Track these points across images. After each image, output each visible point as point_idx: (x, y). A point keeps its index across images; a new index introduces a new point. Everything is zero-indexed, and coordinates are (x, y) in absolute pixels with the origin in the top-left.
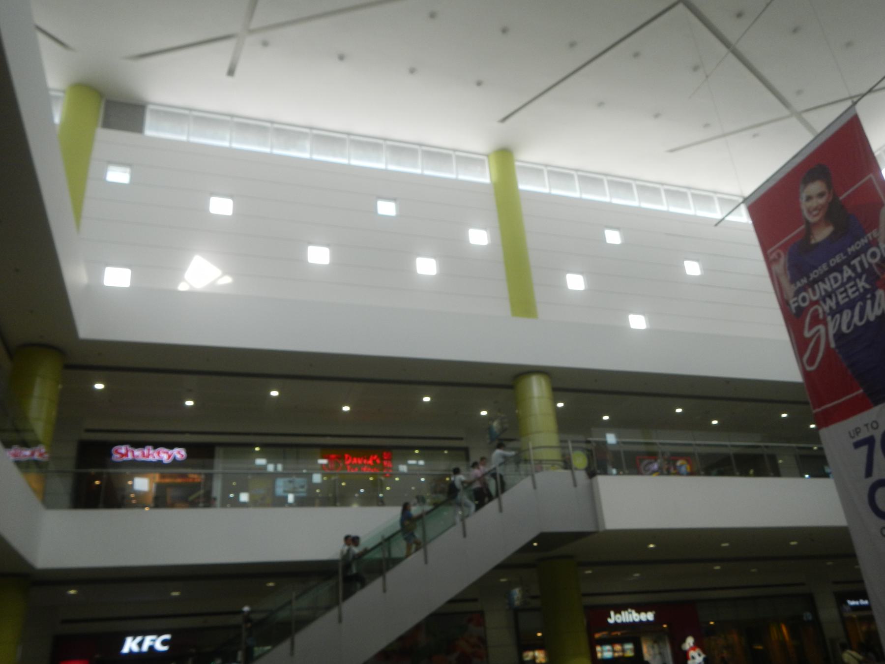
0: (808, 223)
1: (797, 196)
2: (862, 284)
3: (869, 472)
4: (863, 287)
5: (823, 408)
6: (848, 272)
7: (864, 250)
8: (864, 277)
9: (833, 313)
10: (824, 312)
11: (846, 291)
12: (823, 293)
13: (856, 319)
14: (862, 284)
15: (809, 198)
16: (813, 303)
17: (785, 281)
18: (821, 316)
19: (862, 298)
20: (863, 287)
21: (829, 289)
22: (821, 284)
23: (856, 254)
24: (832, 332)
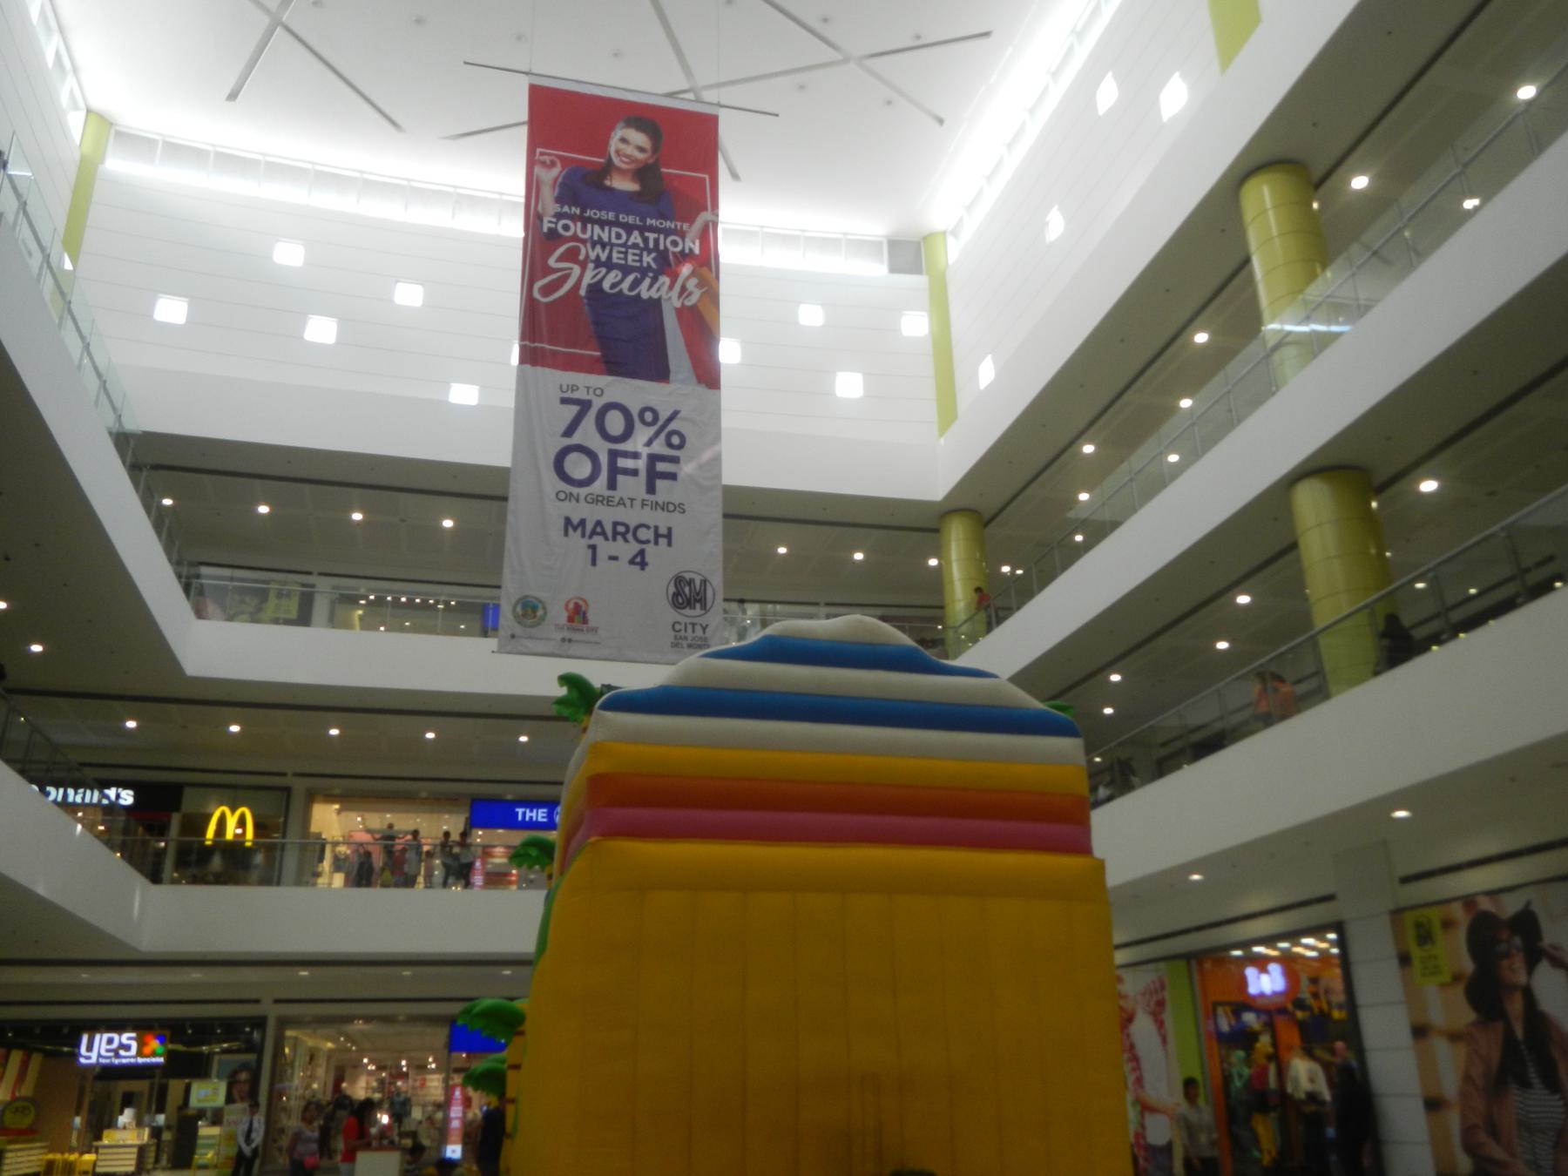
0: (610, 160)
1: (612, 128)
2: (648, 259)
3: (569, 432)
4: (648, 263)
5: (536, 344)
6: (636, 238)
7: (667, 232)
8: (653, 255)
10: (587, 256)
11: (626, 253)
12: (596, 238)
13: (625, 286)
14: (648, 259)
15: (624, 140)
16: (575, 238)
17: (548, 195)
18: (582, 257)
19: (644, 271)
20: (648, 263)
21: (606, 239)
22: (597, 229)
23: (652, 229)
24: (587, 280)
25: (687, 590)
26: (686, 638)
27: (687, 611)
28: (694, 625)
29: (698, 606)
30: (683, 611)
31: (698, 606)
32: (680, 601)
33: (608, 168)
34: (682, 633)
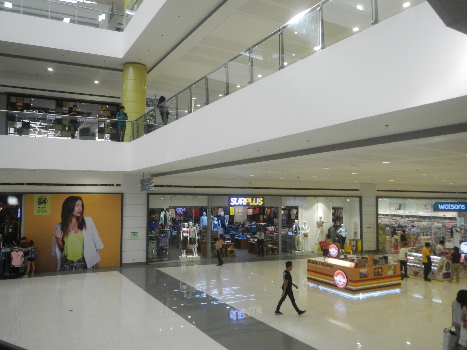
25: (41, 200)
26: (41, 210)
27: (41, 205)
28: (43, 207)
29: (44, 203)
30: (41, 205)
31: (44, 203)
32: (40, 203)
34: (40, 210)
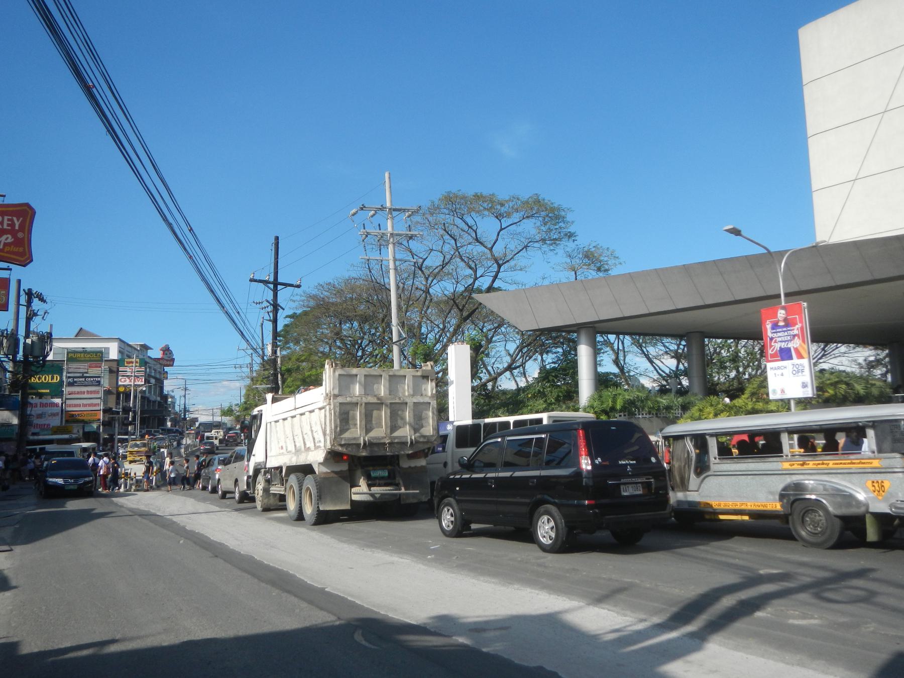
6: (786, 334)
9: (781, 342)
15: (780, 313)
16: (776, 337)
23: (789, 330)
33: (778, 321)
